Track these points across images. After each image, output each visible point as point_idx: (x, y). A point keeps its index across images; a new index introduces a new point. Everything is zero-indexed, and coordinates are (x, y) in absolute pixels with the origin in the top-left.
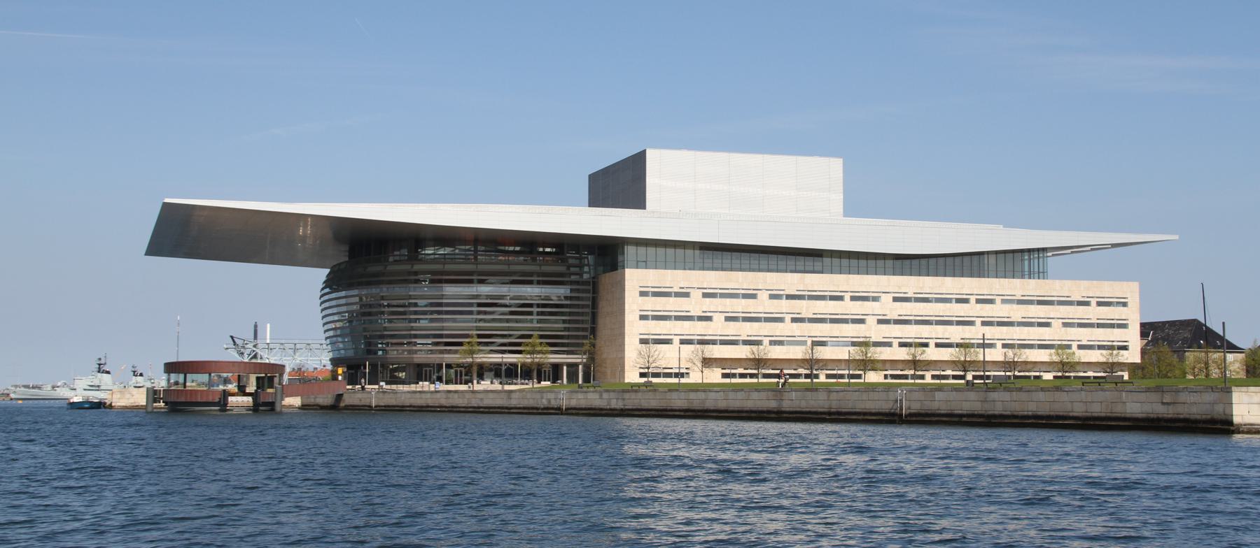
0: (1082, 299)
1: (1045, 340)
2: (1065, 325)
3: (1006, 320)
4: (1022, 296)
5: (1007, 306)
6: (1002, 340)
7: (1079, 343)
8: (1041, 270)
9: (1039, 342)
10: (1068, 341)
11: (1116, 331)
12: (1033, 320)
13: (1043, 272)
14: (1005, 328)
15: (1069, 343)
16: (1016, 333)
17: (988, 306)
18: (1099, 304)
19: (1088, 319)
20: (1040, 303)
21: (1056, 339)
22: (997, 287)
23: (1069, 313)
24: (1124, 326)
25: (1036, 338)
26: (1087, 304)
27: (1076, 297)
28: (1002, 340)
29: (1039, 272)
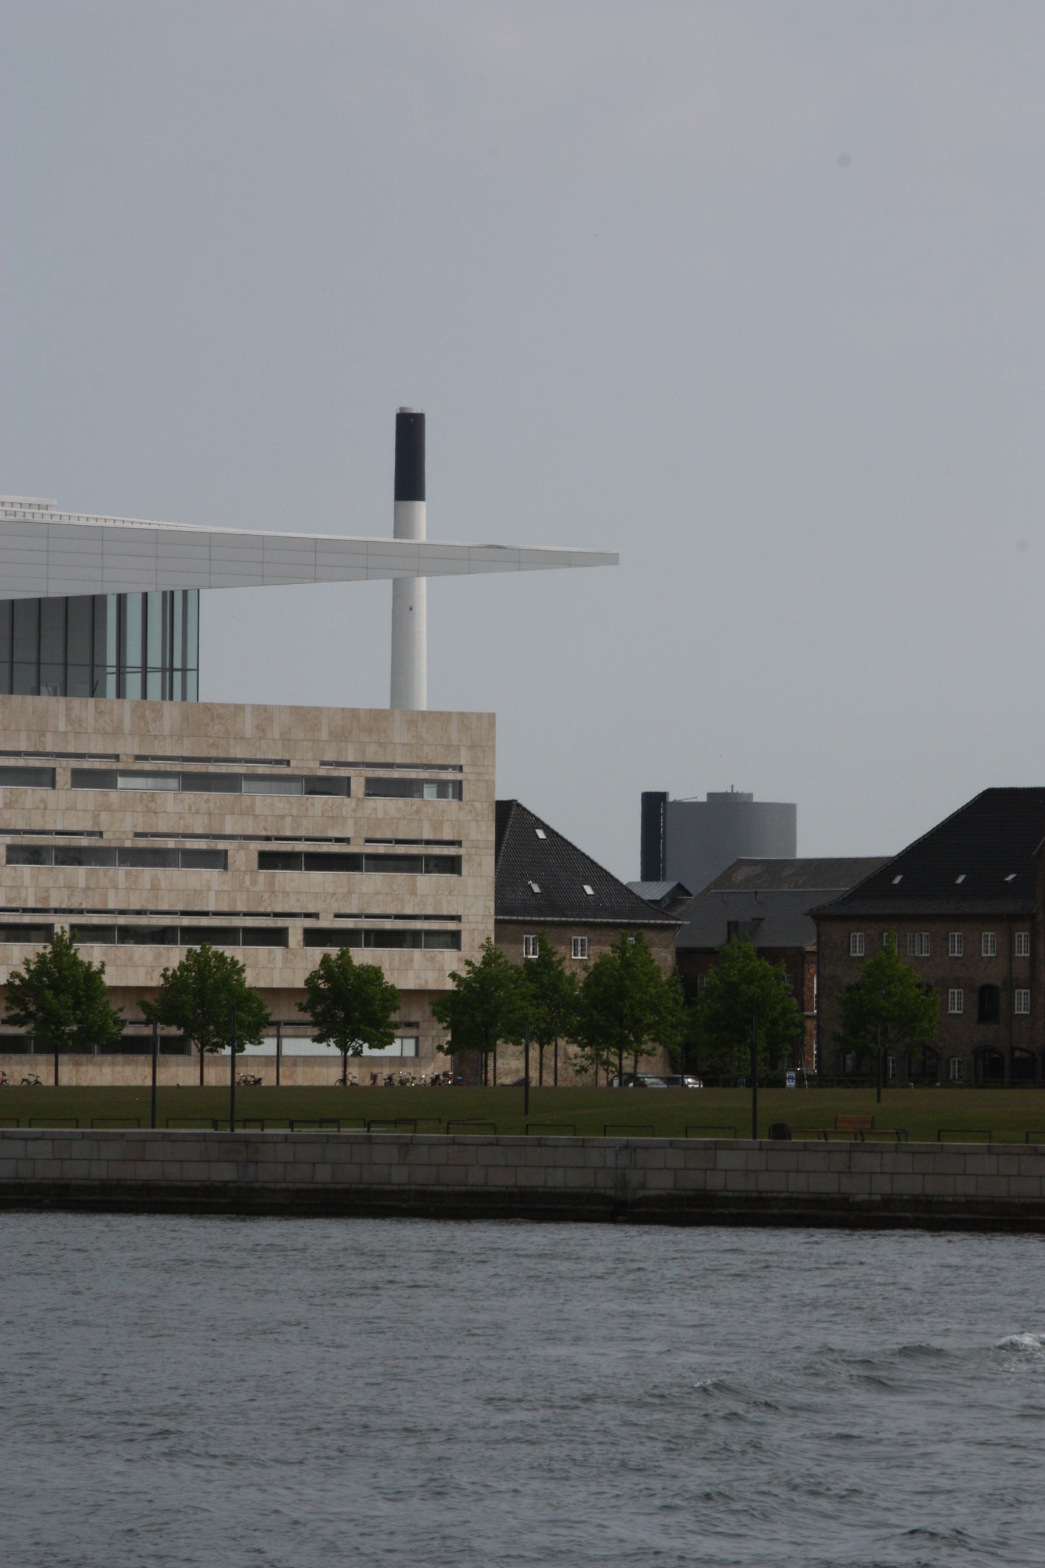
0: (323, 772)
1: (205, 914)
2: (268, 860)
3: (84, 842)
4: (139, 758)
5: (89, 796)
6: (71, 911)
7: (310, 923)
8: (178, 664)
9: (186, 921)
10: (277, 915)
11: (426, 882)
12: (171, 844)
13: (184, 670)
14: (79, 873)
15: (280, 923)
16: (117, 888)
17: (31, 795)
18: (376, 788)
19: (339, 840)
20: (193, 782)
21: (240, 907)
22: (62, 728)
23: (283, 817)
24: (452, 865)
25: (180, 907)
26: (337, 787)
27: (305, 764)
28: (71, 911)
29: (168, 670)
